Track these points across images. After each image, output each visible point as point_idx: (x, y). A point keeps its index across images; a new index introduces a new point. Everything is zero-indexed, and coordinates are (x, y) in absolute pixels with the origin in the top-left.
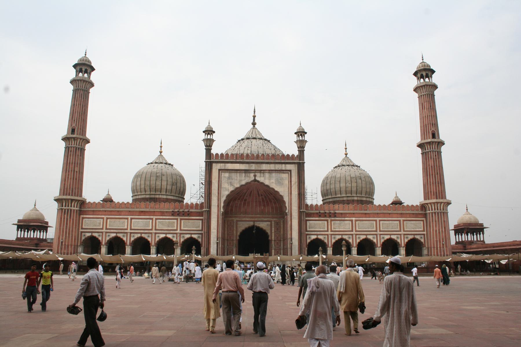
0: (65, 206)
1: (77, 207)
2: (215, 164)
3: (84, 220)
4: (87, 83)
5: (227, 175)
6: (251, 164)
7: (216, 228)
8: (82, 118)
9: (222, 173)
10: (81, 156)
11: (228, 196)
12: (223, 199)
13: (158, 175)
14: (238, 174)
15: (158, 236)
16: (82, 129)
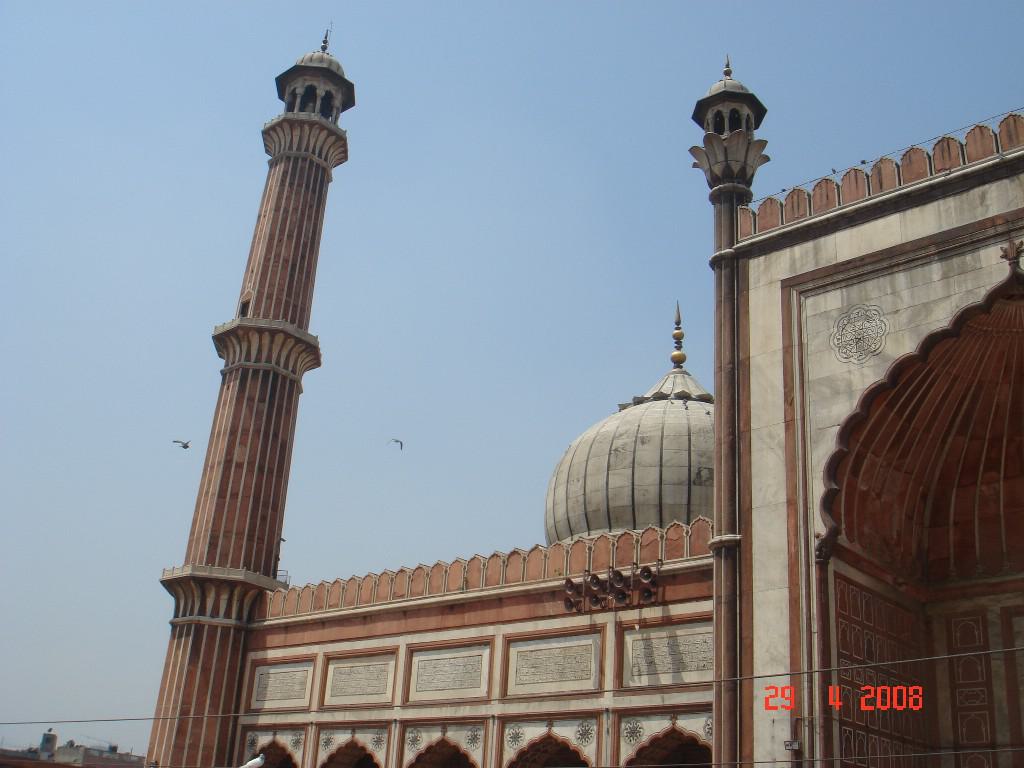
0: (184, 615)
1: (228, 615)
2: (762, 258)
3: (260, 670)
4: (307, 128)
5: (832, 301)
6: (977, 191)
7: (784, 650)
8: (278, 256)
9: (803, 298)
10: (262, 400)
11: (850, 430)
12: (823, 449)
13: (618, 443)
14: (901, 278)
15: (516, 737)
16: (274, 297)
